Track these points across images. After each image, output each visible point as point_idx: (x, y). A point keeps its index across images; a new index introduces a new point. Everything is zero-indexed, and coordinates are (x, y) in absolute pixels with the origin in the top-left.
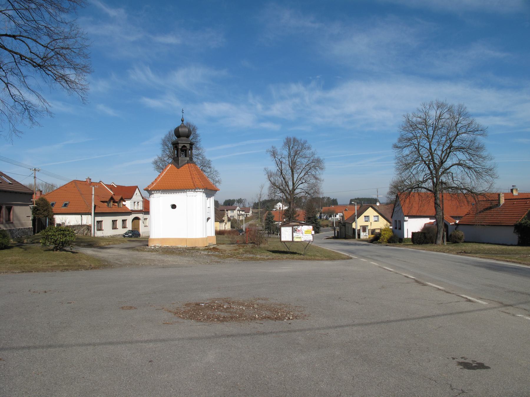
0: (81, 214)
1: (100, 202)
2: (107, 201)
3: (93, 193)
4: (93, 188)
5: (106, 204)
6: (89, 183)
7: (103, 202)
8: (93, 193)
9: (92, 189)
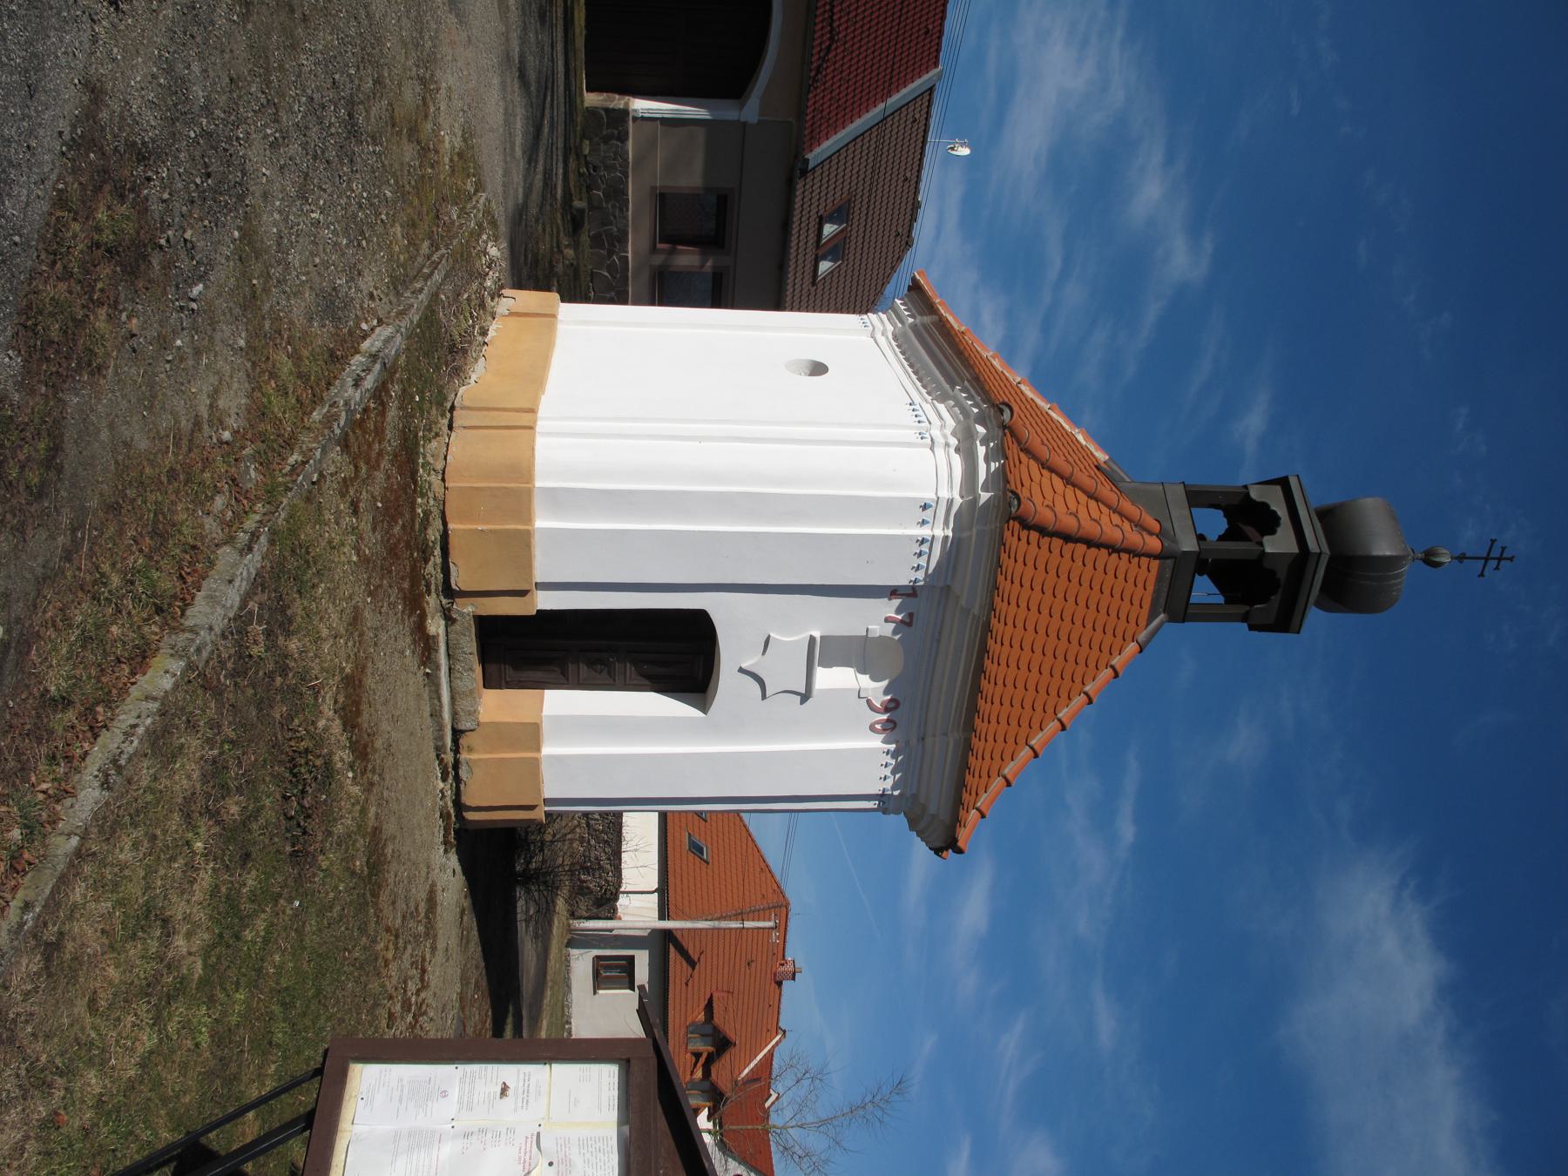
0: (663, 890)
1: (708, 996)
2: (712, 1018)
3: (748, 924)
4: (770, 924)
5: (701, 1017)
6: (780, 907)
7: (709, 1007)
8: (748, 924)
9: (764, 920)
